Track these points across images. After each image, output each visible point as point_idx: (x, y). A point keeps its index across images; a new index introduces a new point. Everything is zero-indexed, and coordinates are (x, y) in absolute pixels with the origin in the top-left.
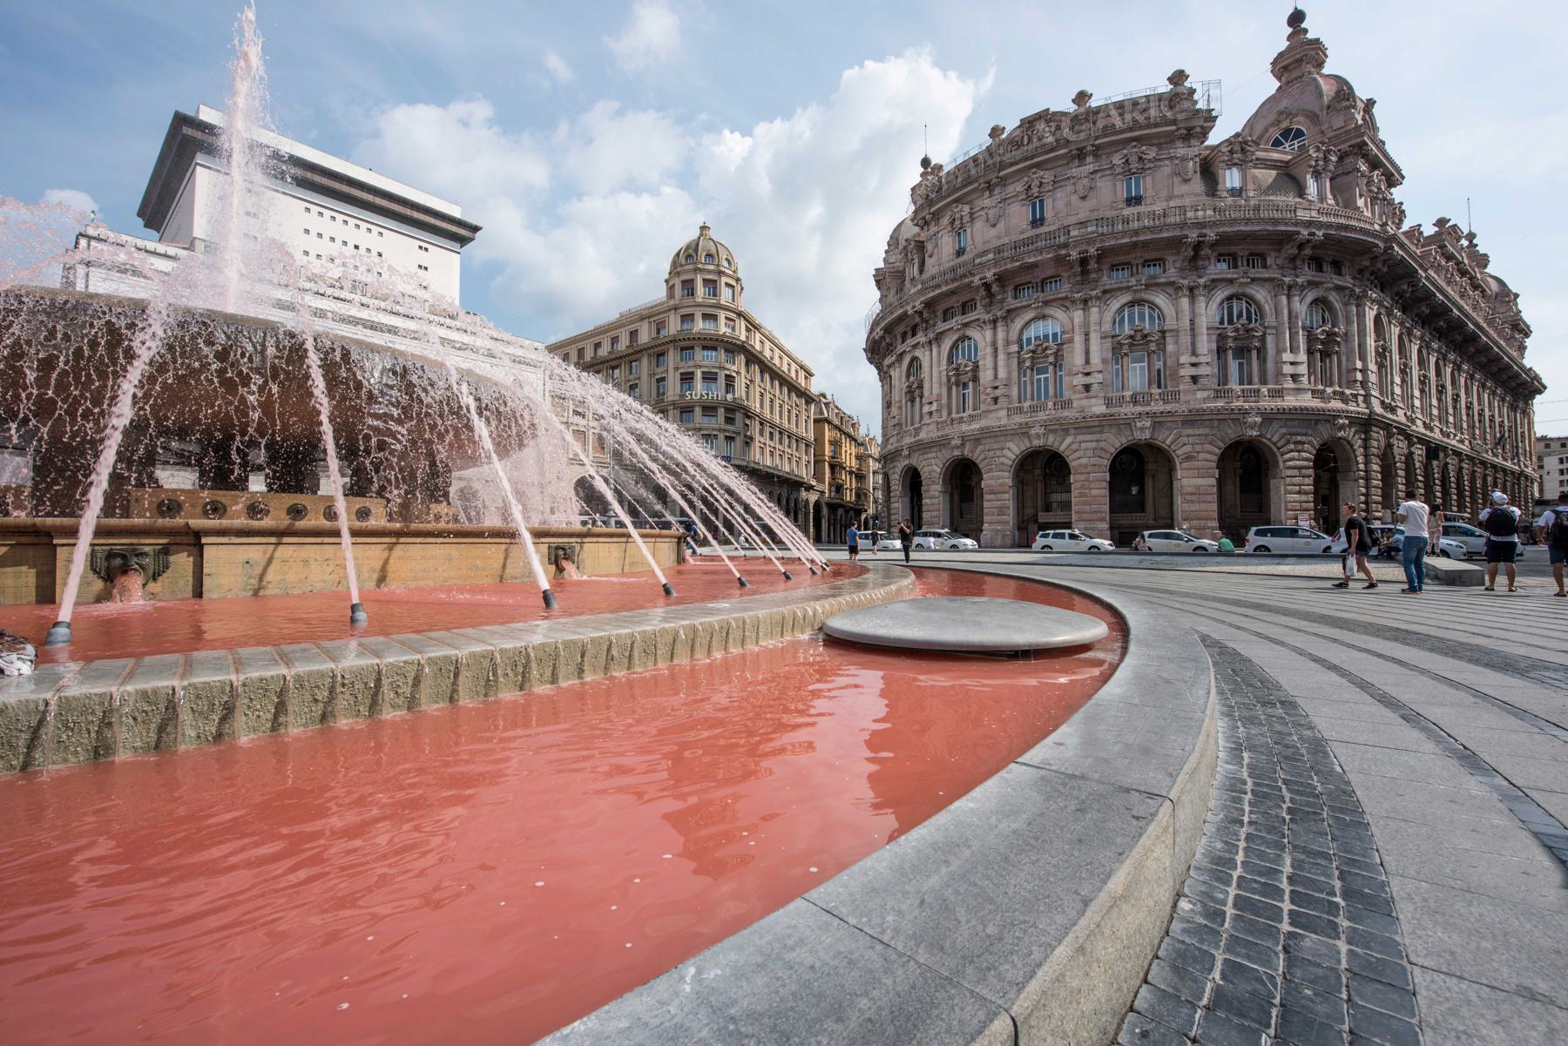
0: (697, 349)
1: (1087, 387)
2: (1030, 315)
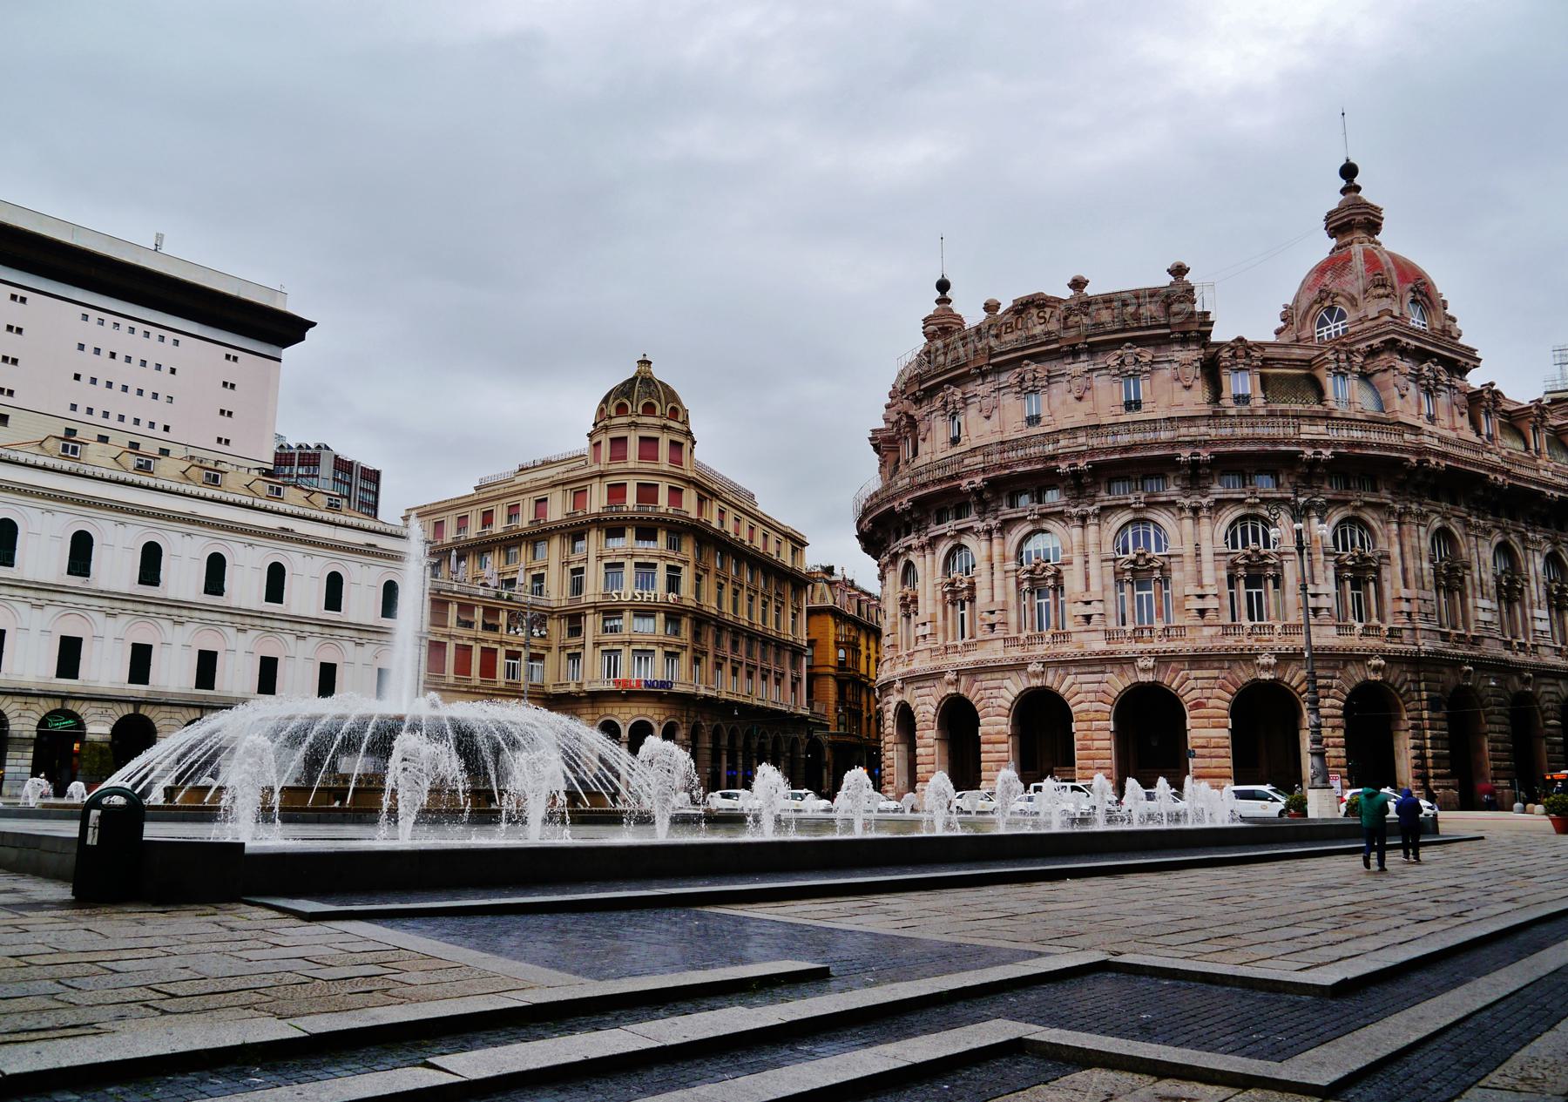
0: (626, 614)
1: (1088, 618)
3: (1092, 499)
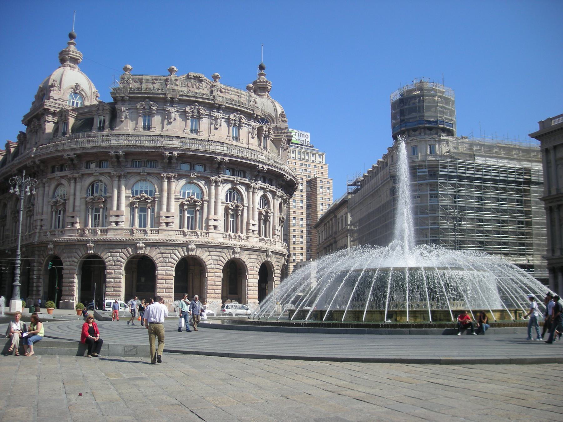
1: (215, 227)
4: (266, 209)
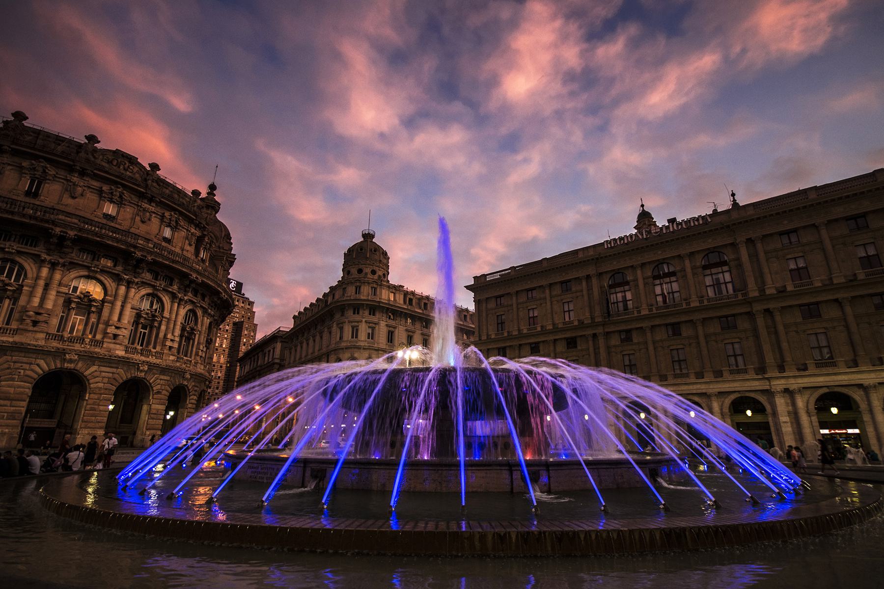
2: (86, 273)
3: (136, 274)
4: (192, 324)
